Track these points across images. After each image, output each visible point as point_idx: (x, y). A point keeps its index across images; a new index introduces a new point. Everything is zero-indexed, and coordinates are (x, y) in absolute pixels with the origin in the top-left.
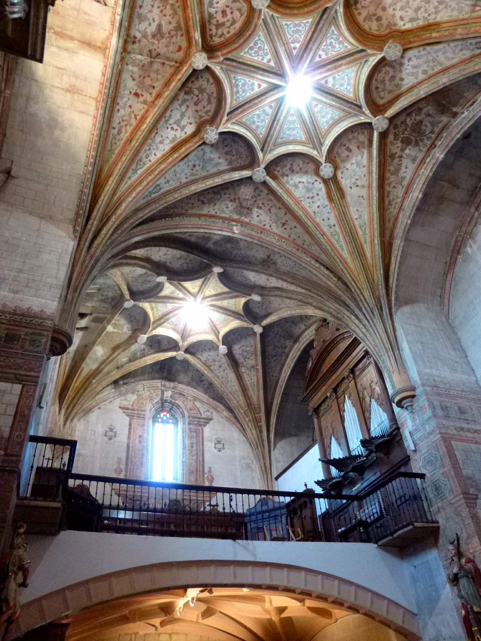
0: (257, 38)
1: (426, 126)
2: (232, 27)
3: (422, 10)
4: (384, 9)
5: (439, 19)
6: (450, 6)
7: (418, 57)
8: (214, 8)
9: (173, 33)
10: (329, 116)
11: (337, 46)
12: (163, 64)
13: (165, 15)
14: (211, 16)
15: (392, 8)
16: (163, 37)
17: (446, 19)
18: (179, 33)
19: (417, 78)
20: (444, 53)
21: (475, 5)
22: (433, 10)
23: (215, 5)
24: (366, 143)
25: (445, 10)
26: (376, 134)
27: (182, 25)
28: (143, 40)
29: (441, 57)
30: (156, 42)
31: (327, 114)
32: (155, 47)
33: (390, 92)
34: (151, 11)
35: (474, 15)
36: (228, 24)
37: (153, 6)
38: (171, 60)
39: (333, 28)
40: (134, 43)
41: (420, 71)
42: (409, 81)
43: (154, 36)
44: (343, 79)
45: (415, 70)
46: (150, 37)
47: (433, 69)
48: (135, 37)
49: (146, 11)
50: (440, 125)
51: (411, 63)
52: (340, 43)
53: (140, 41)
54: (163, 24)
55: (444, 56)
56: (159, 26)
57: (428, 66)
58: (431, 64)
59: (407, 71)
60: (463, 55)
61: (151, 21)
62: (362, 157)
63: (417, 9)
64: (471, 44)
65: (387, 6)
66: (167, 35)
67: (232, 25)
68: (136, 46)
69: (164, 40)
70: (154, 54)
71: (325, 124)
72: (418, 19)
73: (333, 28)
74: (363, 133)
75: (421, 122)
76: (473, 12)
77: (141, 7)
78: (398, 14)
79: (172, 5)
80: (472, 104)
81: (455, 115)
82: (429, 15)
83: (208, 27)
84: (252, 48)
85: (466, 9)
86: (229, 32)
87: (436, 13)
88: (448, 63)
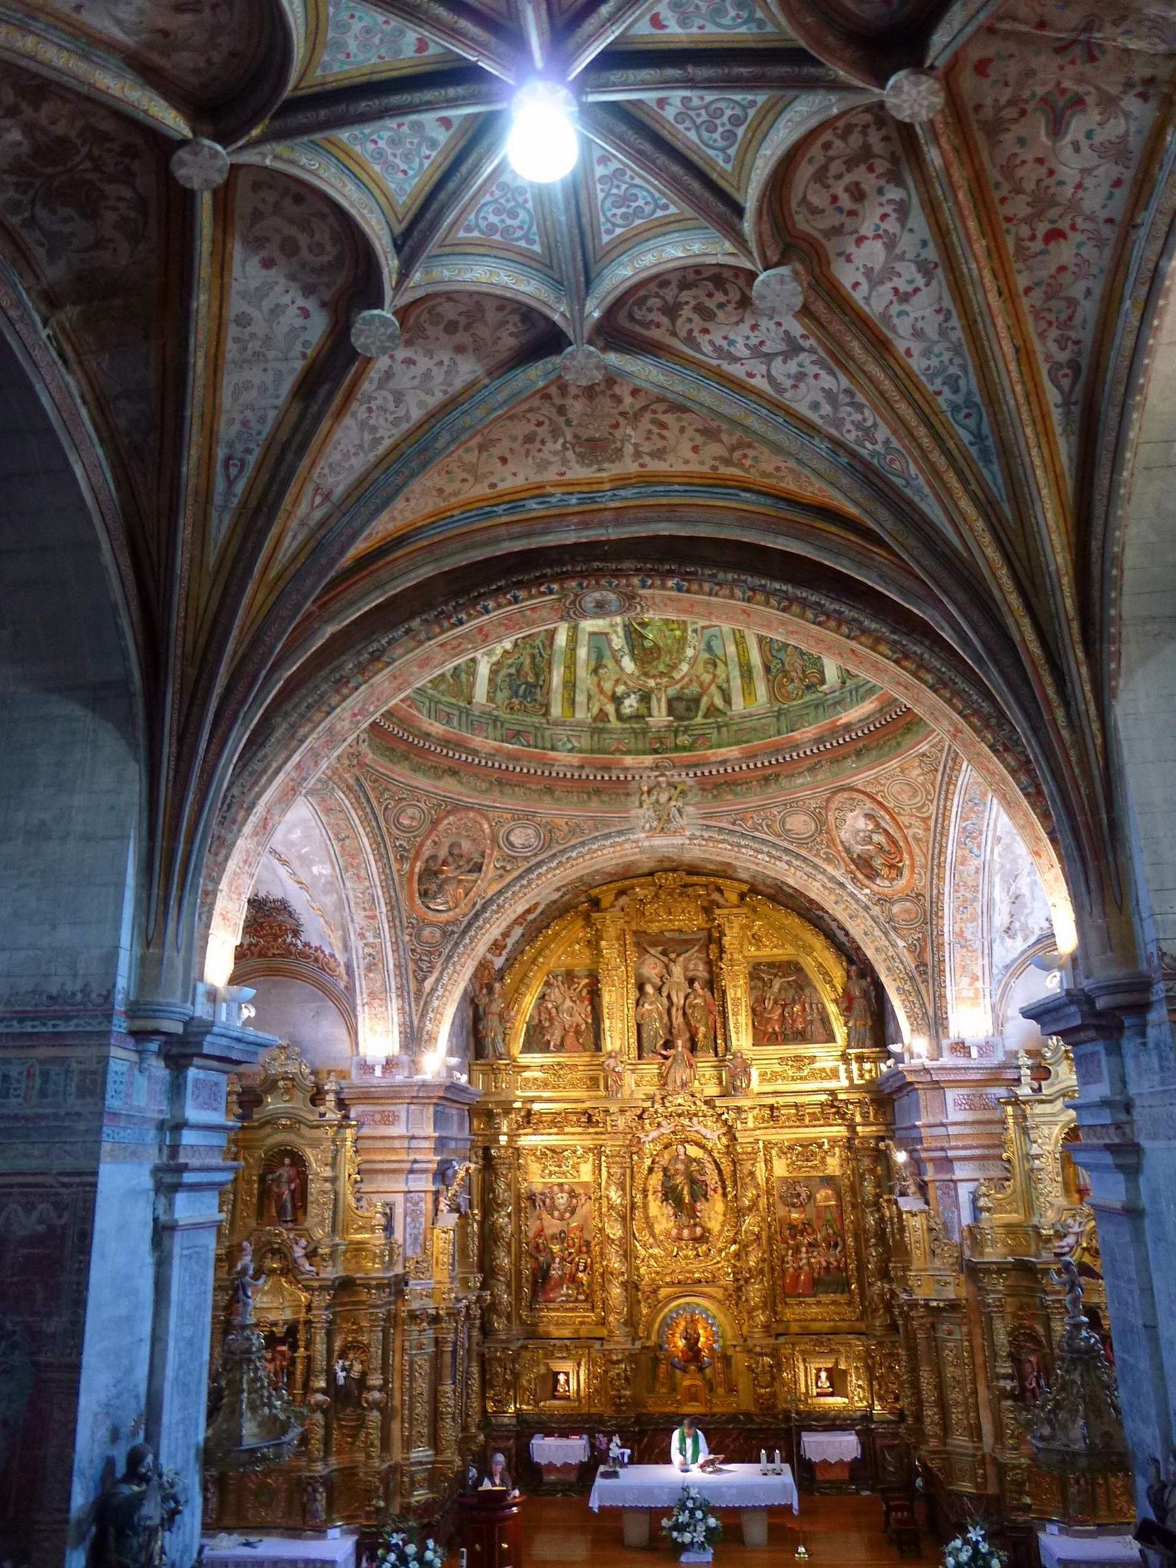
0: (732, 151)
1: (67, 220)
2: (821, 160)
3: (391, 406)
4: (460, 349)
5: (348, 421)
6: (356, 454)
7: (294, 333)
8: (890, 201)
9: (1012, 112)
10: (352, 46)
11: (493, 219)
12: (1042, 25)
13: (1040, 161)
14: (895, 177)
15: (447, 362)
16: (1043, 100)
17: (338, 434)
18: (988, 112)
19: (244, 295)
20: (263, 388)
21: (327, 497)
22: (372, 422)
23: (888, 209)
24: (155, 58)
25: (357, 442)
26: (172, 121)
27: (980, 138)
28: (1114, 90)
29: (254, 375)
30: (1066, 84)
31: (365, 46)
32: (1070, 70)
33: (257, 215)
34: (1085, 172)
35: (309, 489)
36: (835, 168)
37: (1079, 186)
38: (1008, 35)
39: (537, 248)
40: (1150, 81)
41: (255, 313)
42: (247, 271)
43: (1078, 102)
44: (407, 157)
45: (267, 305)
46: (1090, 100)
47: (237, 340)
48: (1143, 96)
49: (1100, 171)
50: (40, 253)
51: (293, 310)
52: (492, 228)
53: (1128, 85)
54: (1044, 139)
55: (256, 382)
56: (1057, 129)
57: (253, 335)
58: (255, 345)
59: (279, 289)
60: (231, 422)
61: (1084, 144)
62: (118, 22)
63: (399, 398)
64: (248, 451)
65: (459, 359)
66: (1030, 107)
67: (825, 168)
68: (1142, 71)
69: (1040, 91)
70: (1077, 50)
71: (344, 15)
72: (380, 387)
73: (537, 248)
74: (196, 71)
75: (91, 213)
76: (317, 489)
77: (1117, 183)
78: (424, 363)
79: (1018, 191)
80: (61, 355)
81: (51, 300)
82: (370, 410)
83: (898, 147)
84: (736, 121)
85: (331, 480)
86: (827, 146)
87: (363, 425)
88: (229, 381)
